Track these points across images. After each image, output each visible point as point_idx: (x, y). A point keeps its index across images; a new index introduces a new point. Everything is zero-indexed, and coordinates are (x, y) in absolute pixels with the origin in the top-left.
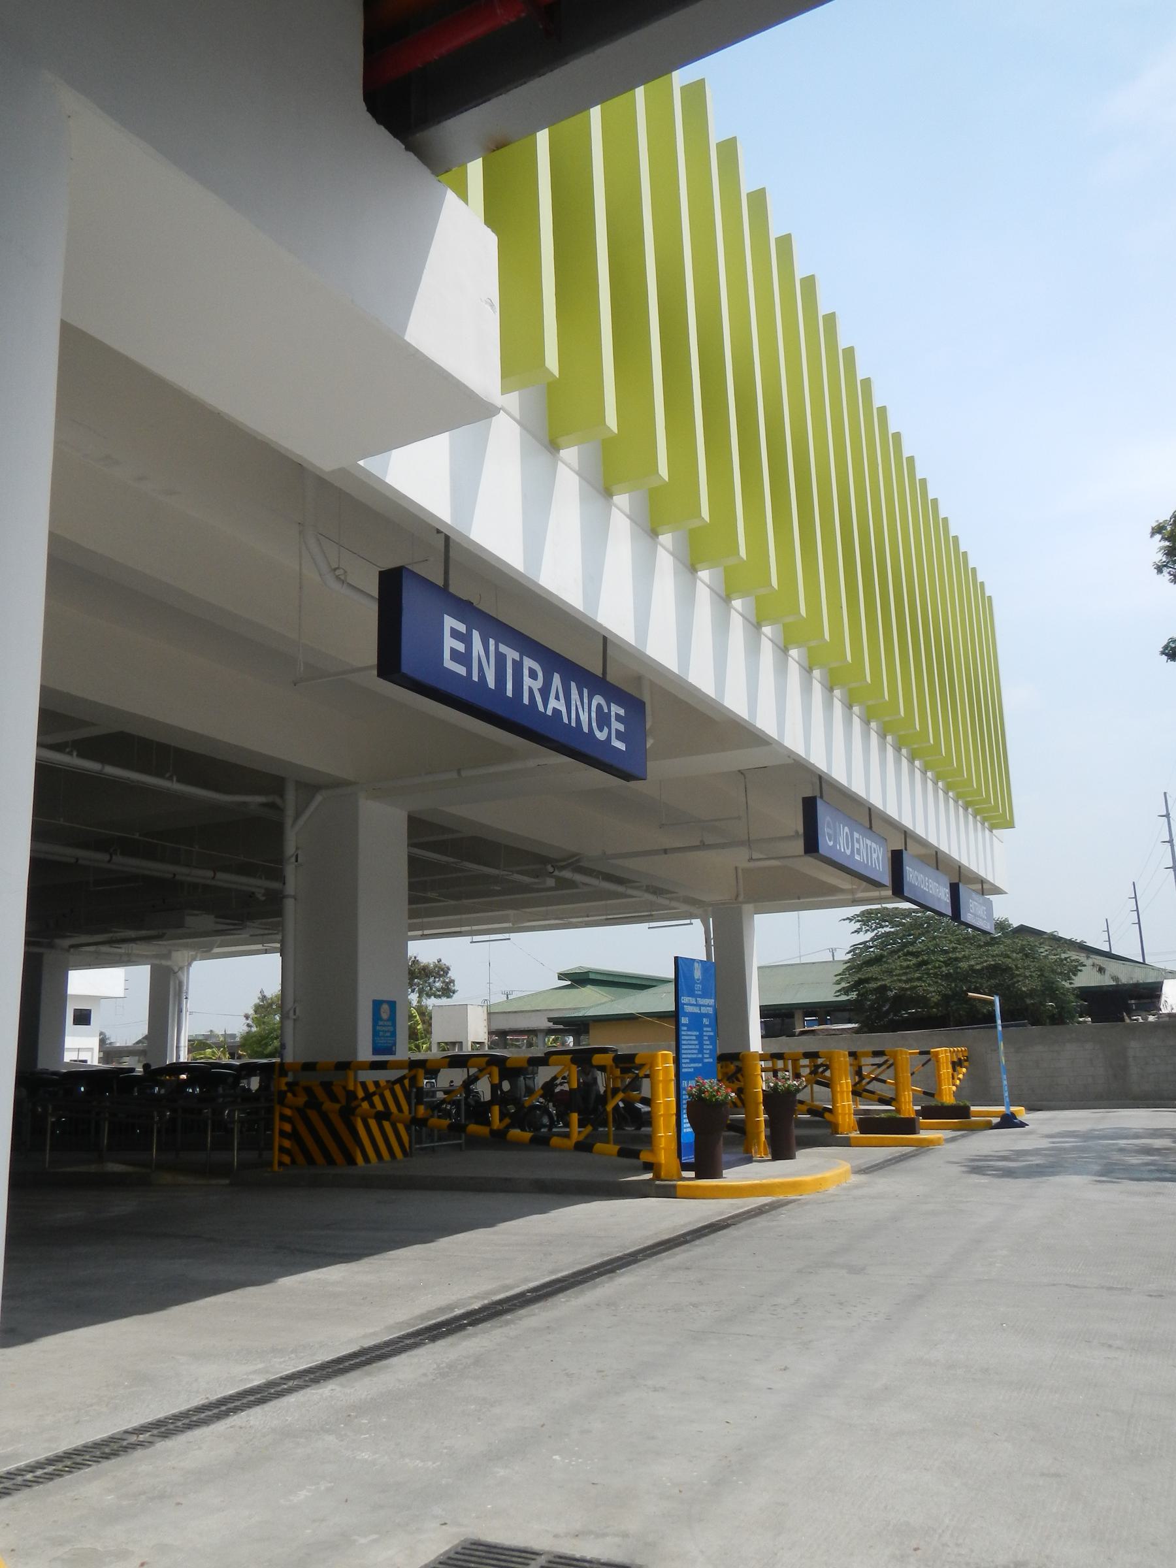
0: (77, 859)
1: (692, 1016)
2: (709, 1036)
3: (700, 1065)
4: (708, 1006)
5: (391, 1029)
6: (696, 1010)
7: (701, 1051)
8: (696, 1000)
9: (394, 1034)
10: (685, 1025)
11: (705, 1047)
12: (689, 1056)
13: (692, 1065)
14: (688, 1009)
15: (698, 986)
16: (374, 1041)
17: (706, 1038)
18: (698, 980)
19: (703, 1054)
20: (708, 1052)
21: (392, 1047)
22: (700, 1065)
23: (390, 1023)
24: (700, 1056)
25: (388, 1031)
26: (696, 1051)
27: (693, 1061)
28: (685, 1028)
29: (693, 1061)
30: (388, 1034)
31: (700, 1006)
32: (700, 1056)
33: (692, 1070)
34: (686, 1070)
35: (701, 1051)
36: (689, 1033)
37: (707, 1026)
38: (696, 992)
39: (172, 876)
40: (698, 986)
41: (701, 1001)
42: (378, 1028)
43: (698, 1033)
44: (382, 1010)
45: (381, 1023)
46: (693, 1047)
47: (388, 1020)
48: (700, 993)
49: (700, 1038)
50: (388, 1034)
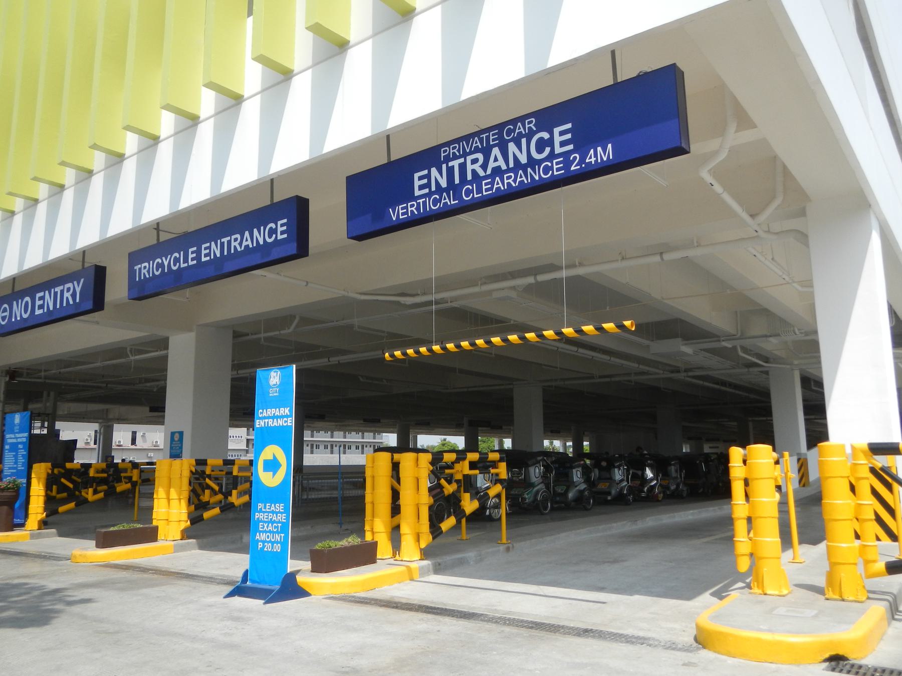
0: (339, 361)
1: (12, 444)
2: (23, 455)
3: (15, 471)
4: (23, 437)
5: (180, 445)
6: (14, 441)
7: (16, 463)
8: (15, 436)
9: (181, 448)
10: (7, 450)
11: (19, 461)
12: (8, 466)
13: (10, 471)
14: (10, 441)
15: (16, 429)
16: (170, 451)
17: (21, 456)
18: (17, 424)
19: (17, 465)
20: (21, 463)
21: (179, 454)
22: (15, 471)
23: (179, 442)
24: (15, 466)
25: (178, 446)
26: (13, 463)
27: (10, 468)
28: (7, 451)
29: (10, 468)
30: (178, 448)
31: (17, 438)
32: (15, 466)
33: (10, 473)
34: (6, 473)
35: (16, 463)
36: (9, 454)
37: (22, 449)
38: (15, 431)
39: (337, 362)
40: (16, 429)
41: (17, 435)
42: (172, 445)
43: (14, 453)
44: (175, 437)
45: (174, 443)
46: (11, 461)
47: (178, 441)
48: (18, 431)
49: (16, 457)
50: (178, 448)
